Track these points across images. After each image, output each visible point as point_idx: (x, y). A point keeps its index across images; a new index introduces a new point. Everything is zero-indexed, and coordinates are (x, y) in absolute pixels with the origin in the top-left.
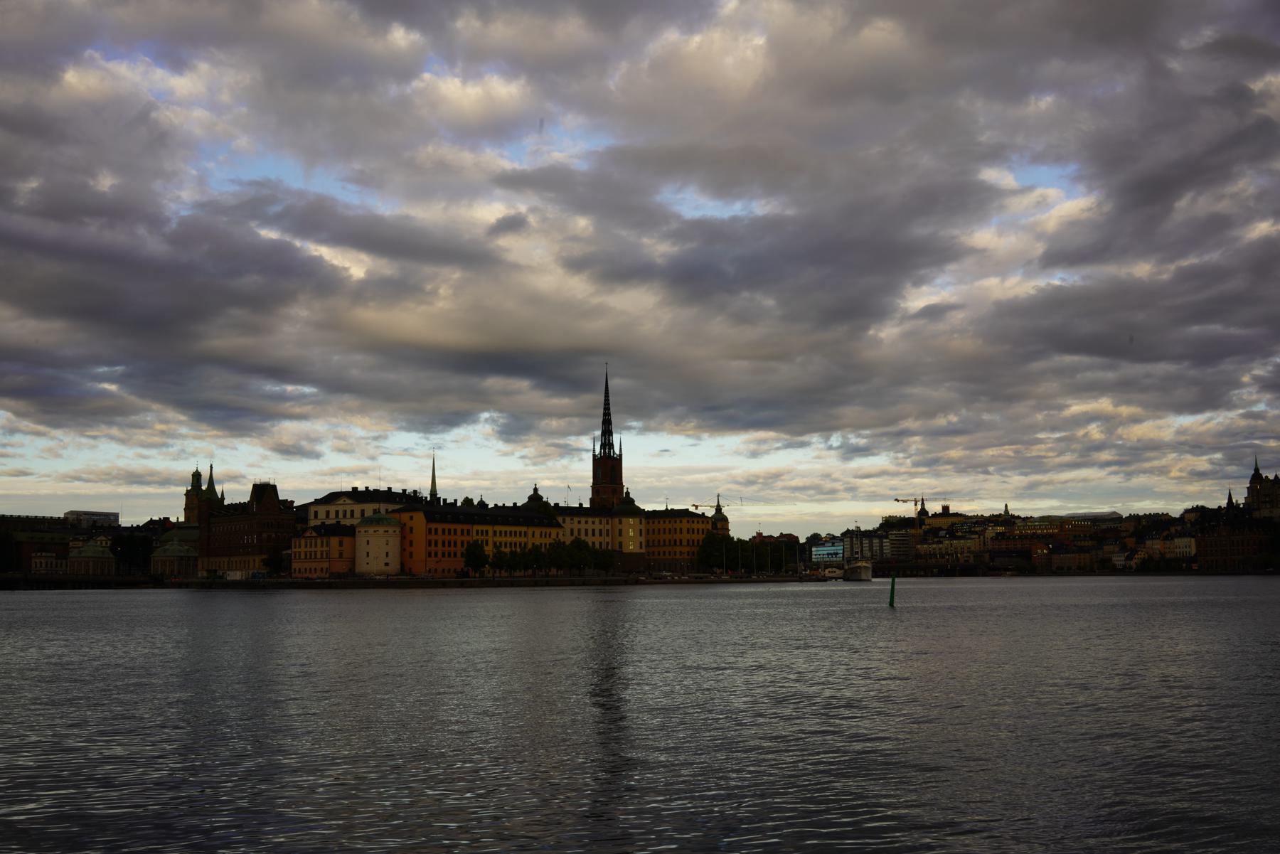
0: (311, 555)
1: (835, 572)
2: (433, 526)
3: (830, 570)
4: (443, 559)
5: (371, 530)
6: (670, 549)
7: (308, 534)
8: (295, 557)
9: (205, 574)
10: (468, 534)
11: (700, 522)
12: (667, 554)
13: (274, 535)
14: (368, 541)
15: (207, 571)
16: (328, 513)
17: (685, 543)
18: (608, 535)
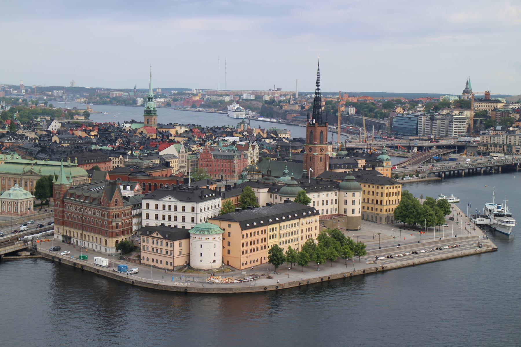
0: (157, 250)
1: (483, 220)
2: (245, 232)
3: (480, 218)
4: (251, 254)
5: (204, 238)
6: (373, 206)
7: (155, 235)
8: (144, 248)
9: (61, 238)
10: (265, 233)
11: (395, 187)
12: (370, 209)
13: (120, 224)
14: (201, 245)
15: (63, 236)
16: (157, 206)
17: (384, 203)
18: (336, 203)
